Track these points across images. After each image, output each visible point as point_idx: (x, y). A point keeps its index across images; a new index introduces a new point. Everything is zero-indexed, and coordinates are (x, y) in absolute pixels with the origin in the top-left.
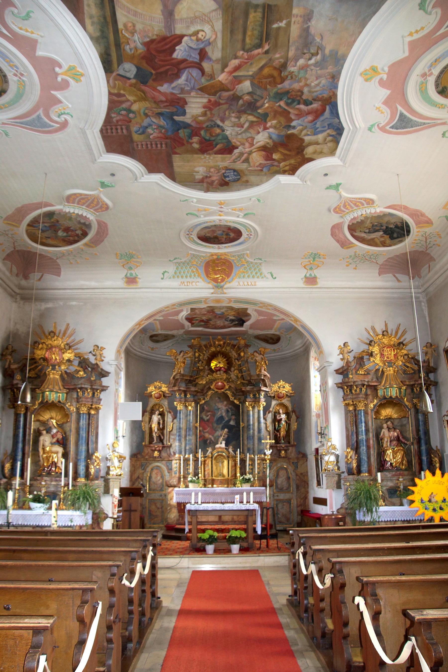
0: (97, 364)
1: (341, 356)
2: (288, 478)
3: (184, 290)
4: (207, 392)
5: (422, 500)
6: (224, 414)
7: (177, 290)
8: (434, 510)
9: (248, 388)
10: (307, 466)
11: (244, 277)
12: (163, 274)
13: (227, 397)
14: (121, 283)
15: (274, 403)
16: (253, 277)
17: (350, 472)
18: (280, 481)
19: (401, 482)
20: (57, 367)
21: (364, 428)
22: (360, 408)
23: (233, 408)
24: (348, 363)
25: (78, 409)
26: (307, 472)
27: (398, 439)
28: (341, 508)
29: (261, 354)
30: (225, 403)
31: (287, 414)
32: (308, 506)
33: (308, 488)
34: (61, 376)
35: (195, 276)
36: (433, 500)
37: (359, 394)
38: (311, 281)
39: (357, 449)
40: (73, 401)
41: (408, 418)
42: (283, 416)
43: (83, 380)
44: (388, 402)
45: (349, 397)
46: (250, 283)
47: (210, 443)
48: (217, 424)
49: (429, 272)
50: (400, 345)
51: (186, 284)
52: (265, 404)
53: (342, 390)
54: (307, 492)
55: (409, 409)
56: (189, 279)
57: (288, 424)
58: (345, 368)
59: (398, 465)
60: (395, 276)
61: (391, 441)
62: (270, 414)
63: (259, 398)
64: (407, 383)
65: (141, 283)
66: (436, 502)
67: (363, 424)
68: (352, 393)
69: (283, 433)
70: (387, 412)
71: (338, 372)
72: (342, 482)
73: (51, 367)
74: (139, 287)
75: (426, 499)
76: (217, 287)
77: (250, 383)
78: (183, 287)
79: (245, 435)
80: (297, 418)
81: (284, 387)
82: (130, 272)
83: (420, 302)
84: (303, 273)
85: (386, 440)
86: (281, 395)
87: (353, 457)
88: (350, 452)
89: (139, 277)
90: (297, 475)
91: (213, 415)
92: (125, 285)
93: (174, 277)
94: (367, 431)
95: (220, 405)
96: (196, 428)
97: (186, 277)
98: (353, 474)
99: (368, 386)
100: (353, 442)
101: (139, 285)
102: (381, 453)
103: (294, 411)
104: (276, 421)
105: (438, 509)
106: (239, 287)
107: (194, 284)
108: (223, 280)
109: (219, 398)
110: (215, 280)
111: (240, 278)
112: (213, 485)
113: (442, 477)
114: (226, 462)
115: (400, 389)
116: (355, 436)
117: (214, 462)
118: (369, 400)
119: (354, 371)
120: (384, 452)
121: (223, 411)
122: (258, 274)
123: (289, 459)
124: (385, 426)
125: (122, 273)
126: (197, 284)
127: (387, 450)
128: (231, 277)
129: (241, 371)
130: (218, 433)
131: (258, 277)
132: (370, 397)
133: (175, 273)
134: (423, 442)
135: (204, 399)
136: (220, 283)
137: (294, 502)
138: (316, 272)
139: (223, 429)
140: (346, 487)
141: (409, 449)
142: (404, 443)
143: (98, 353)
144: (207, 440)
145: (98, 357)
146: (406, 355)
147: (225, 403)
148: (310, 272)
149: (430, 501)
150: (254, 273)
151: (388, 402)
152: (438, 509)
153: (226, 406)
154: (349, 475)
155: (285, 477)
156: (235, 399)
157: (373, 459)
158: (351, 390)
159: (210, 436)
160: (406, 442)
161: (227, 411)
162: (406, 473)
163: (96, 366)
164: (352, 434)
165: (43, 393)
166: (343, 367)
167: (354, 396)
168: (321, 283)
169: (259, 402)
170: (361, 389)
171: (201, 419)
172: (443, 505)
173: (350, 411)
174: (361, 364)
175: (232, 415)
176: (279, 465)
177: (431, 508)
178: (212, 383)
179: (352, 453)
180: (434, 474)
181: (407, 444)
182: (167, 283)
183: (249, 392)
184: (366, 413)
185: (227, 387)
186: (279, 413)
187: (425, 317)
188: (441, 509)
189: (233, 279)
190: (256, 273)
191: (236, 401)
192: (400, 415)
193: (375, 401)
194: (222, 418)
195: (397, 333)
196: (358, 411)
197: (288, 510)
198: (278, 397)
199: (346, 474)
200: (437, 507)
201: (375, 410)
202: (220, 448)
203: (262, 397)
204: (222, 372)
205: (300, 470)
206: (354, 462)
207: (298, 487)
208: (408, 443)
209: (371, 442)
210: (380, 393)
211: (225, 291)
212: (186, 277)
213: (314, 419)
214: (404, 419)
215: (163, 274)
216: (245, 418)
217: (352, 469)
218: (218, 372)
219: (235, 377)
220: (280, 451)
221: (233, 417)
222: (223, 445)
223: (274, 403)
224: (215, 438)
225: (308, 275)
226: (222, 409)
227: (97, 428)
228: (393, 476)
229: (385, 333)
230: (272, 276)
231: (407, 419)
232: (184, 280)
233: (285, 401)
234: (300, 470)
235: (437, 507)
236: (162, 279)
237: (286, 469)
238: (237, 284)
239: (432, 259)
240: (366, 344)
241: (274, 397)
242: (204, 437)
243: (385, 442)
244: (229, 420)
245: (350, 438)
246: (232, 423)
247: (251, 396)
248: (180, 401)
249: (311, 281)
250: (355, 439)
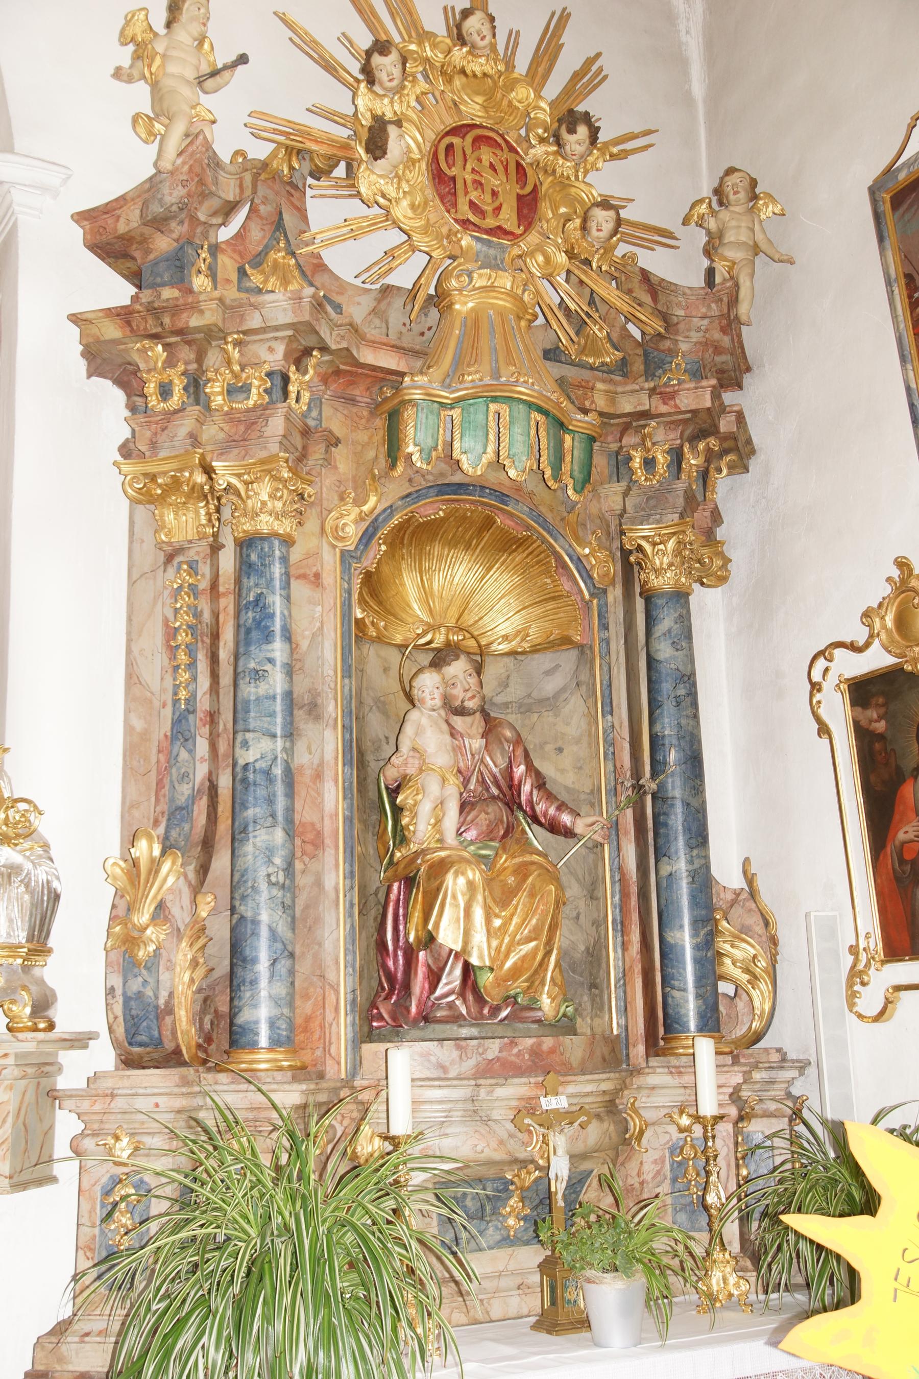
17: (143, 1044)
22: (265, 524)
24: (201, 164)
44: (469, 516)
53: (118, 396)
55: (599, 593)
58: (172, 195)
59: (520, 984)
61: (464, 807)
64: (601, 402)
72: (66, 1125)
85: (433, 787)
87: (180, 913)
88: (155, 866)
98: (172, 1059)
99: (346, 373)
100: (185, 791)
102: (396, 884)
116: (202, 746)
119: (227, 264)
120: (417, 881)
124: (429, 684)
127: (440, 868)
134: (677, 819)
140: (103, 1173)
142: (554, 828)
146: (605, 204)
151: (469, 516)
154: (129, 1062)
157: (336, 937)
158: (195, 386)
160: (566, 819)
164: (180, 732)
166: (152, 185)
174: (279, 225)
179: (172, 876)
181: (569, 833)
187: (682, 63)
192: (522, 633)
193: (373, 500)
196: (246, 544)
199: (102, 1056)
201: (369, 561)
206: (183, 954)
208: (579, 827)
214: (545, 660)
217: (169, 1010)
231: (568, 658)
243: (425, 808)
250: (202, 771)
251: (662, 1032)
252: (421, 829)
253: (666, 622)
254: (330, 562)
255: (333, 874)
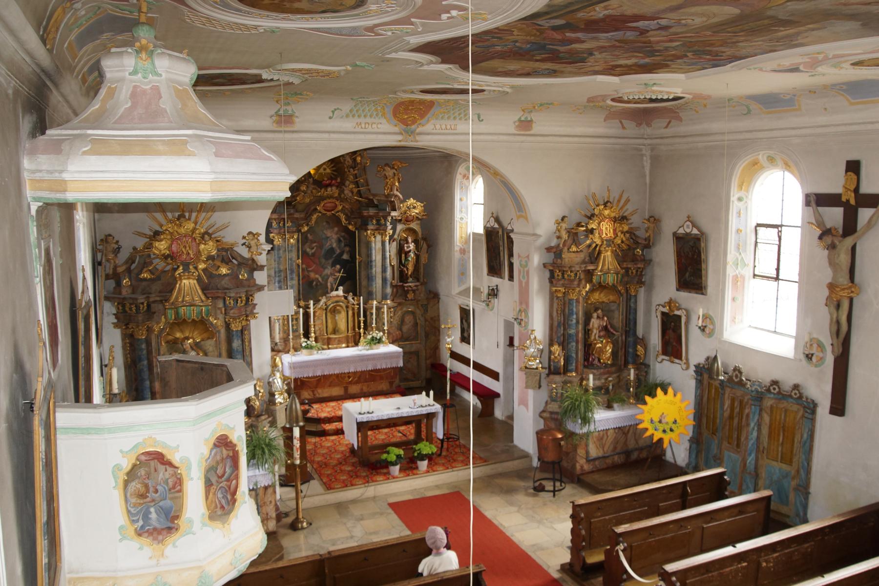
0: (253, 260)
1: (558, 234)
2: (416, 324)
3: (362, 136)
4: (311, 215)
5: (652, 421)
6: (334, 245)
7: (352, 136)
8: (664, 431)
9: (372, 211)
10: (438, 309)
11: (442, 118)
12: (333, 112)
13: (338, 221)
14: (267, 123)
15: (400, 227)
16: (455, 118)
18: (405, 328)
19: (610, 381)
20: (191, 267)
21: (574, 321)
23: (346, 236)
25: (227, 326)
26: (439, 316)
27: (605, 328)
28: (543, 411)
29: (393, 168)
30: (336, 229)
31: (416, 242)
32: (439, 357)
33: (439, 335)
34: (199, 280)
35: (377, 115)
36: (663, 421)
37: (572, 281)
38: (525, 125)
39: (564, 345)
40: (219, 312)
41: (619, 305)
42: (412, 246)
43: (227, 278)
45: (561, 282)
46: (448, 127)
47: (316, 285)
48: (327, 259)
49: (666, 127)
50: (623, 219)
51: (363, 126)
52: (391, 232)
54: (439, 341)
56: (368, 120)
57: (417, 256)
60: (621, 122)
62: (395, 243)
63: (385, 225)
65: (299, 124)
66: (667, 423)
67: (575, 316)
68: (563, 277)
69: (411, 267)
70: (597, 297)
71: (549, 249)
73: (181, 268)
74: (295, 129)
75: (656, 419)
76: (407, 132)
77: (371, 204)
78: (358, 129)
79: (363, 273)
80: (429, 246)
81: (414, 208)
82: (284, 108)
83: (642, 155)
84: (517, 115)
85: (595, 331)
86: (411, 218)
89: (296, 114)
90: (426, 320)
91: (321, 247)
92: (274, 127)
93: (347, 116)
94: (578, 322)
95: (329, 233)
96: (298, 266)
97: (365, 116)
101: (296, 127)
103: (424, 239)
104: (401, 251)
105: (668, 430)
106: (435, 131)
107: (374, 126)
108: (414, 122)
109: (328, 223)
110: (404, 122)
111: (437, 119)
112: (328, 344)
113: (675, 395)
114: (343, 314)
115: (617, 274)
117: (329, 314)
118: (581, 286)
121: (333, 241)
122: (462, 115)
123: (418, 301)
125: (273, 109)
126: (379, 126)
127: (596, 344)
128: (426, 118)
129: (357, 184)
130: (328, 271)
131: (460, 119)
132: (583, 282)
133: (351, 111)
135: (307, 225)
136: (410, 125)
137: (423, 354)
138: (534, 116)
139: (333, 265)
141: (617, 341)
143: (253, 243)
144: (313, 281)
145: (254, 249)
147: (336, 229)
148: (526, 115)
149: (660, 422)
150: (456, 114)
151: (601, 287)
152: (668, 430)
153: (337, 234)
155: (412, 323)
156: (349, 224)
159: (317, 276)
161: (339, 241)
162: (613, 369)
163: (250, 262)
164: (559, 326)
165: (176, 309)
167: (566, 282)
168: (536, 129)
169: (385, 231)
170: (576, 274)
171: (305, 253)
172: (674, 427)
173: (558, 298)
175: (345, 246)
176: (405, 309)
177: (661, 429)
178: (319, 203)
180: (666, 393)
182: (337, 124)
183: (372, 217)
184: (578, 301)
185: (340, 208)
186: (407, 243)
188: (671, 430)
189: (428, 121)
190: (459, 114)
191: (350, 227)
194: (331, 250)
195: (619, 201)
197: (415, 364)
198: (407, 220)
200: (667, 428)
202: (338, 296)
203: (388, 224)
204: (334, 188)
205: (430, 314)
207: (427, 336)
209: (580, 335)
210: (595, 279)
211: (418, 138)
212: (365, 116)
213: (457, 255)
215: (333, 112)
216: (364, 250)
218: (329, 189)
219: (350, 194)
220: (407, 292)
221: (347, 249)
222: (340, 292)
223: (400, 227)
224: (323, 279)
225: (523, 119)
226: (332, 238)
227: (250, 342)
228: (601, 374)
229: (609, 204)
230: (479, 117)
232: (362, 120)
233: (414, 225)
234: (430, 314)
235: (667, 428)
236: (330, 118)
237: (413, 313)
238: (433, 127)
239: (680, 119)
240: (586, 216)
241: (400, 220)
242: (308, 276)
244: (342, 254)
245: (555, 329)
246: (345, 257)
247: (374, 221)
248: (279, 233)
249: (525, 125)
251: (626, 363)
252: (593, 338)
253: (633, 300)
254: (581, 299)
255: (580, 346)
